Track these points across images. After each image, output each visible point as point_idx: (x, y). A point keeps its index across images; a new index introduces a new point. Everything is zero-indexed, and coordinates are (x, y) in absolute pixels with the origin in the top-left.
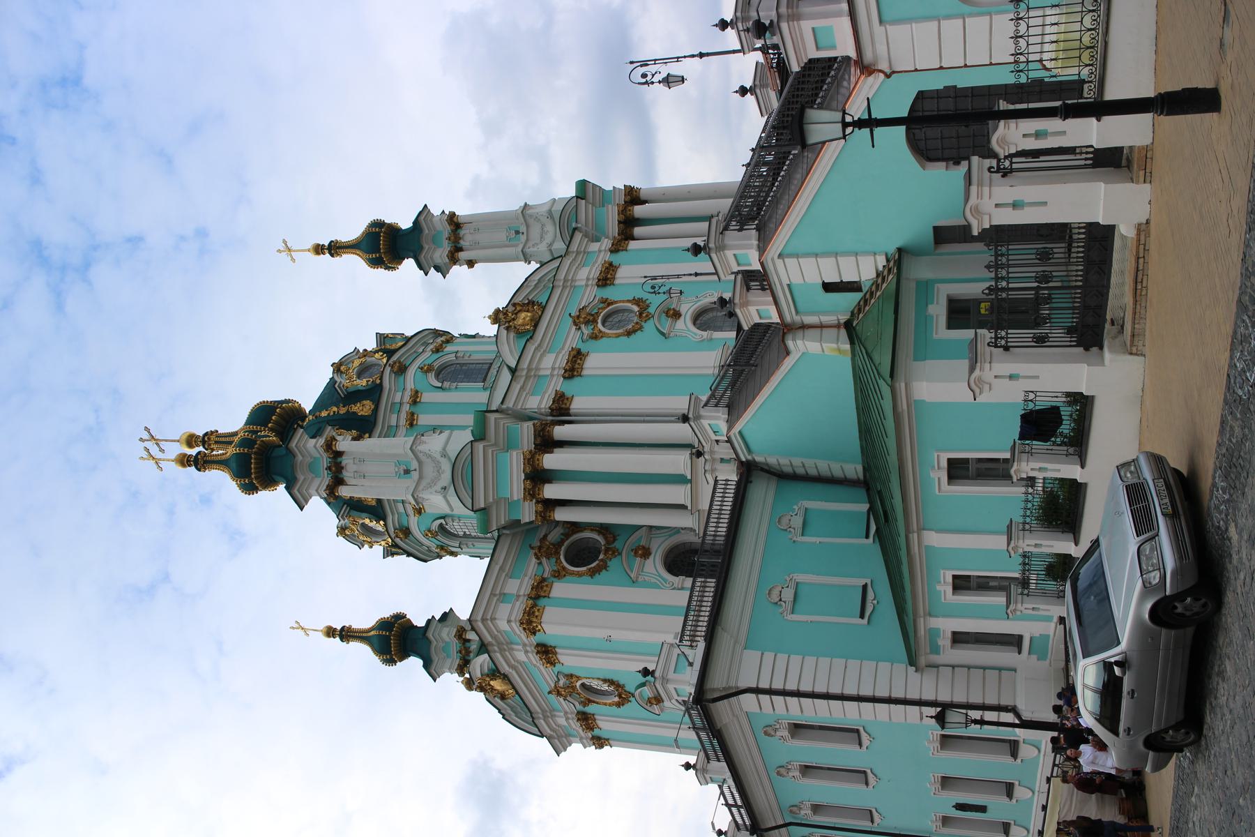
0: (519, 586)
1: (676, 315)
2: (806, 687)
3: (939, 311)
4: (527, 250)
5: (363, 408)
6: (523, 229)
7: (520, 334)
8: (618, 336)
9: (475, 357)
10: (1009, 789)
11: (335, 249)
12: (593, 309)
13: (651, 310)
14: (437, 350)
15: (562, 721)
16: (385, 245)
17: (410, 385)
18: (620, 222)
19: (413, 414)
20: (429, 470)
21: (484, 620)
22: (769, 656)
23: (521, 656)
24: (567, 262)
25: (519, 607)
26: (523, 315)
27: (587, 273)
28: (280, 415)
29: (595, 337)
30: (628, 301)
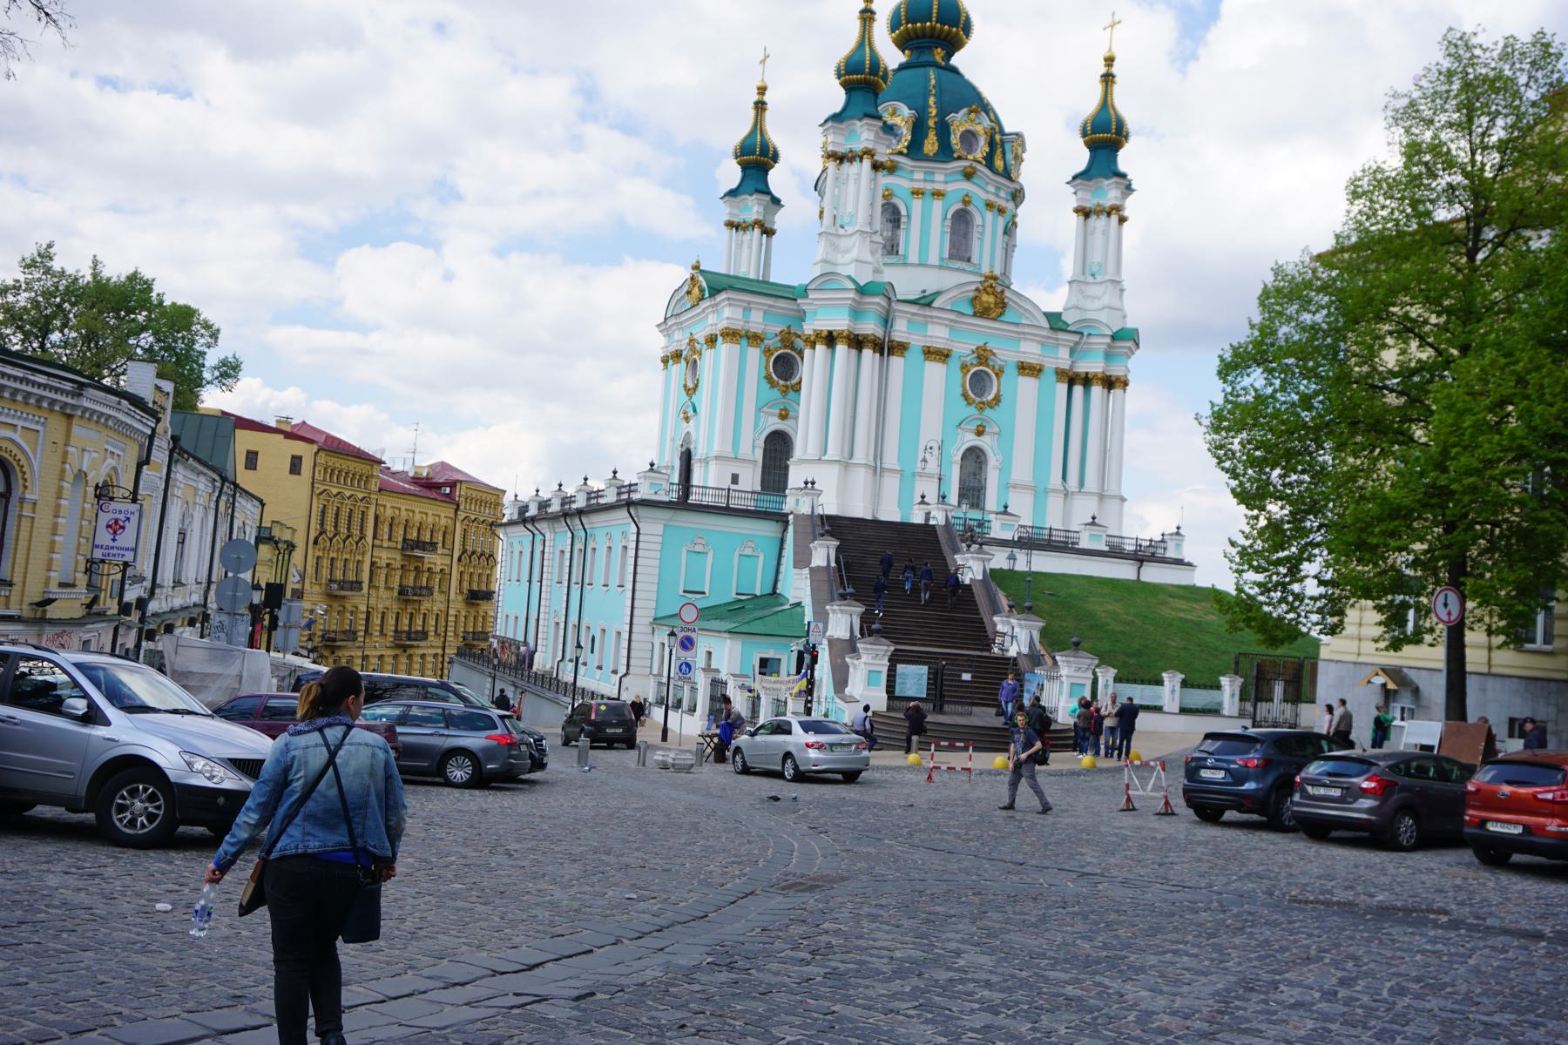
0: (756, 321)
1: (980, 433)
2: (640, 561)
3: (770, 654)
5: (931, 145)
6: (1099, 278)
8: (963, 386)
9: (976, 244)
10: (600, 668)
11: (1108, 79)
13: (988, 412)
14: (989, 205)
15: (677, 336)
16: (1105, 137)
17: (950, 188)
20: (844, 243)
22: (660, 539)
23: (711, 319)
25: (738, 326)
26: (991, 299)
27: (1031, 351)
28: (950, 32)
29: (964, 368)
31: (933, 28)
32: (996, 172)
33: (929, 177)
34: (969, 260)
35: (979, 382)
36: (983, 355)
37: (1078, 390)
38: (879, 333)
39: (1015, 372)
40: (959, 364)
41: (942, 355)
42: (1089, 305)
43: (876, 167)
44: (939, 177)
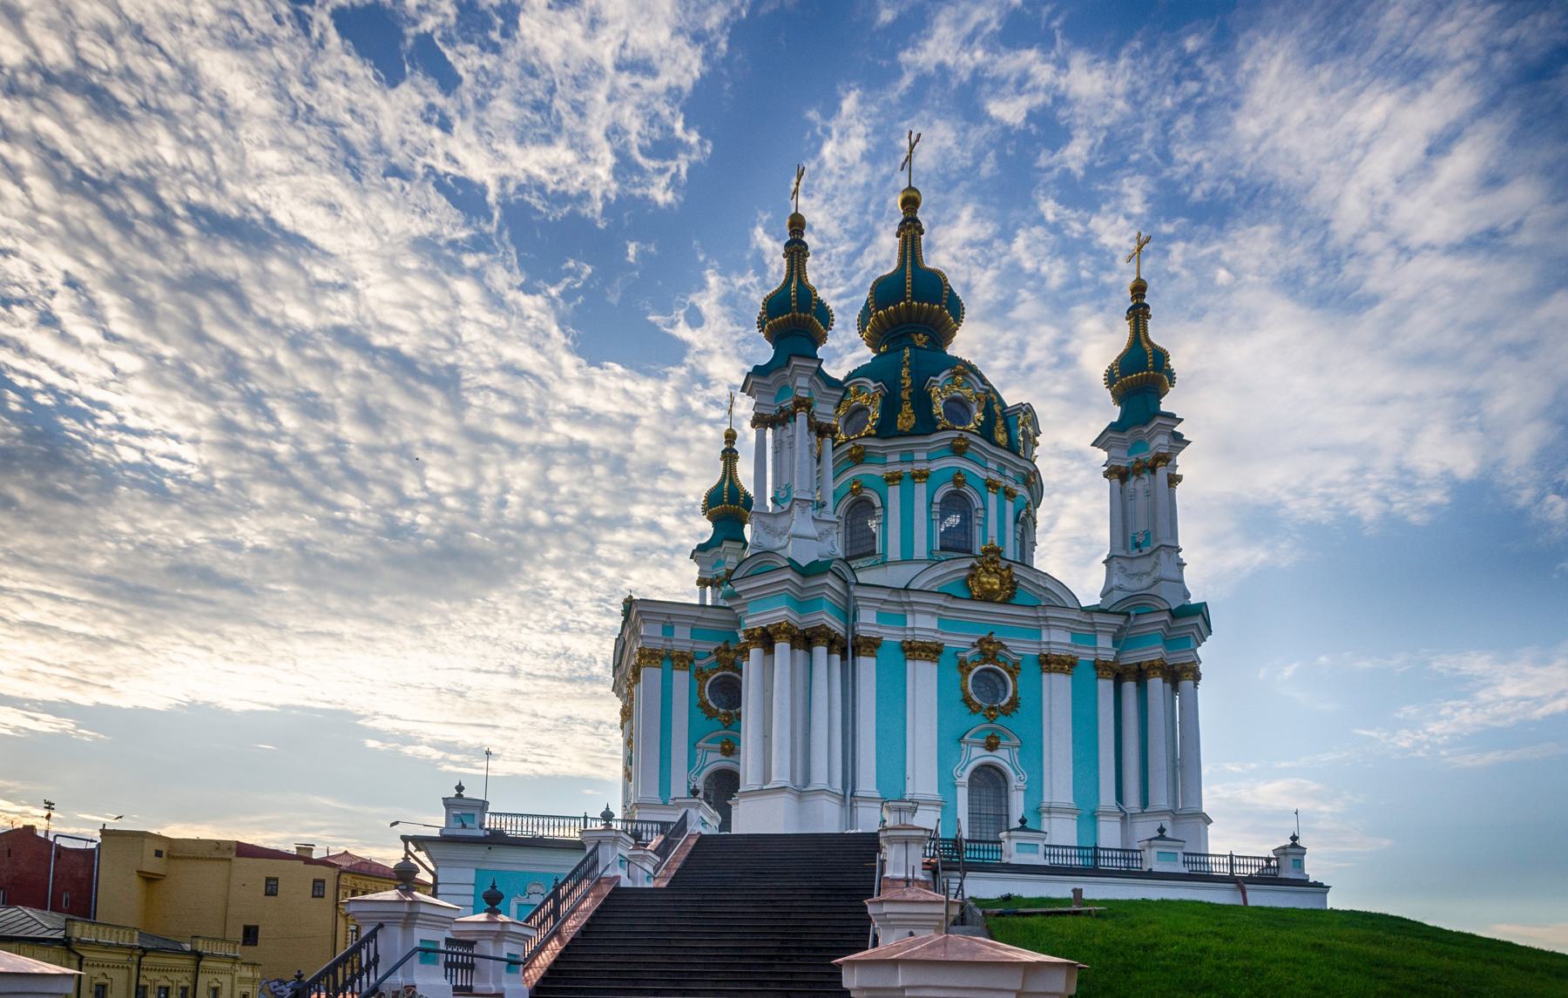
0: (682, 640)
4: (1114, 563)
5: (906, 418)
8: (964, 690)
12: (1003, 656)
13: (1002, 720)
14: (990, 485)
17: (936, 466)
18: (1139, 664)
19: (900, 478)
21: (639, 612)
25: (659, 644)
27: (1058, 640)
28: (931, 311)
29: (963, 666)
30: (1015, 692)
31: (909, 307)
32: (998, 445)
35: (990, 682)
36: (989, 649)
39: (1038, 669)
40: (955, 662)
41: (931, 652)
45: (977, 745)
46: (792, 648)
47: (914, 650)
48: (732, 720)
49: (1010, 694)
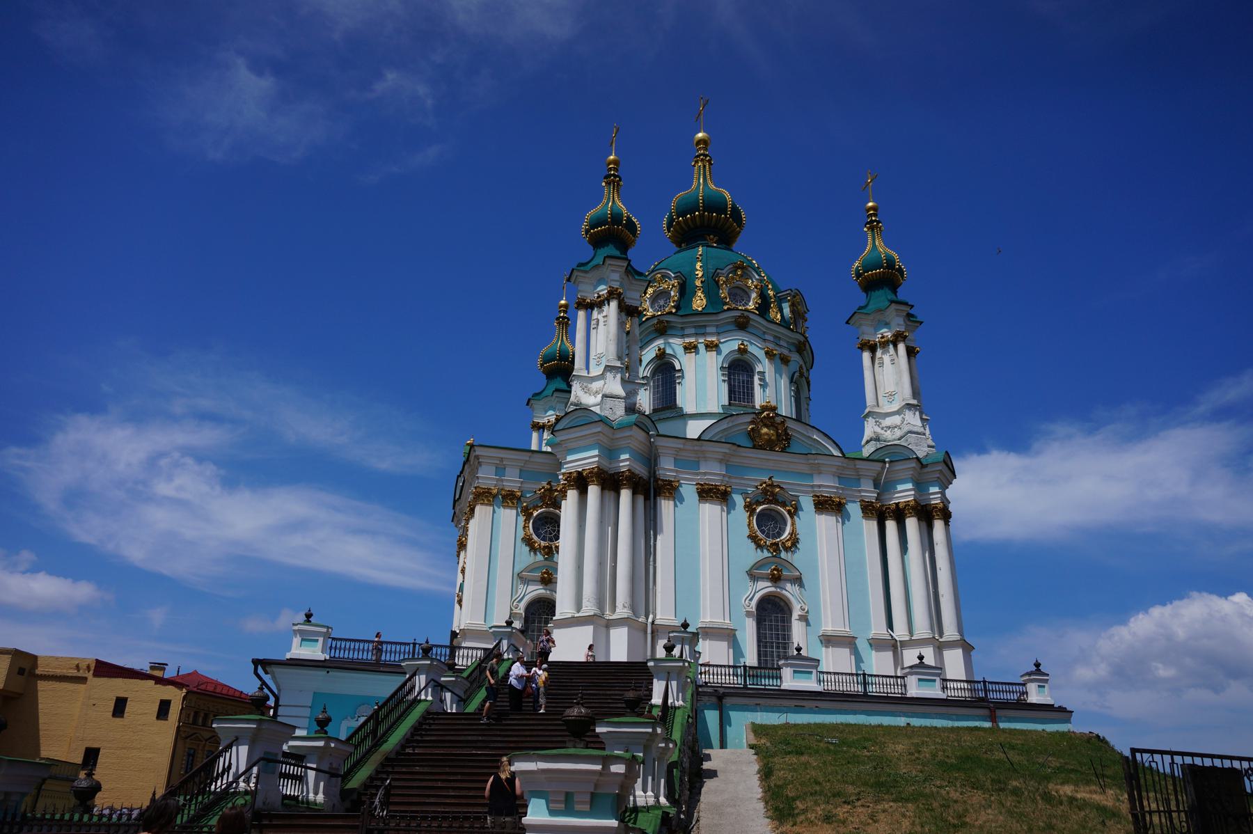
1: (776, 579)
5: (699, 302)
7: (753, 435)
13: (783, 555)
18: (897, 504)
20: (596, 385)
24: (838, 463)
27: (827, 484)
28: (718, 219)
29: (750, 508)
31: (701, 216)
33: (702, 331)
34: (754, 407)
37: (891, 526)
38: (641, 470)
42: (888, 435)
43: (629, 311)
44: (709, 330)
45: (762, 578)
46: (603, 489)
47: (707, 493)
48: (550, 552)
49: (788, 529)
